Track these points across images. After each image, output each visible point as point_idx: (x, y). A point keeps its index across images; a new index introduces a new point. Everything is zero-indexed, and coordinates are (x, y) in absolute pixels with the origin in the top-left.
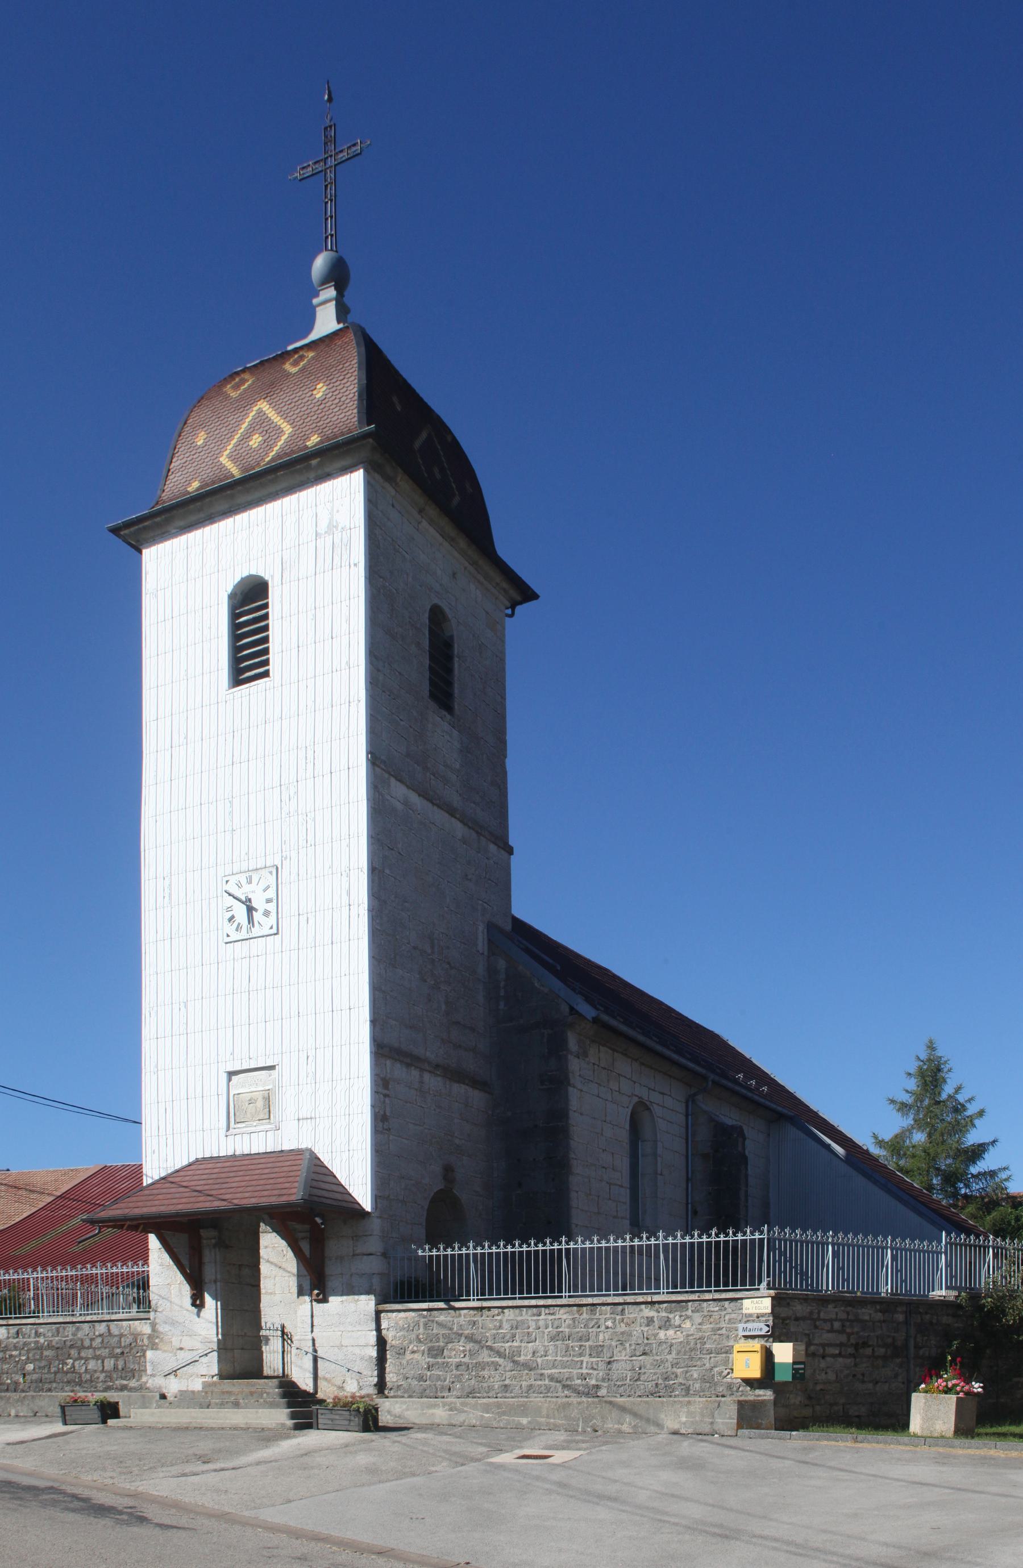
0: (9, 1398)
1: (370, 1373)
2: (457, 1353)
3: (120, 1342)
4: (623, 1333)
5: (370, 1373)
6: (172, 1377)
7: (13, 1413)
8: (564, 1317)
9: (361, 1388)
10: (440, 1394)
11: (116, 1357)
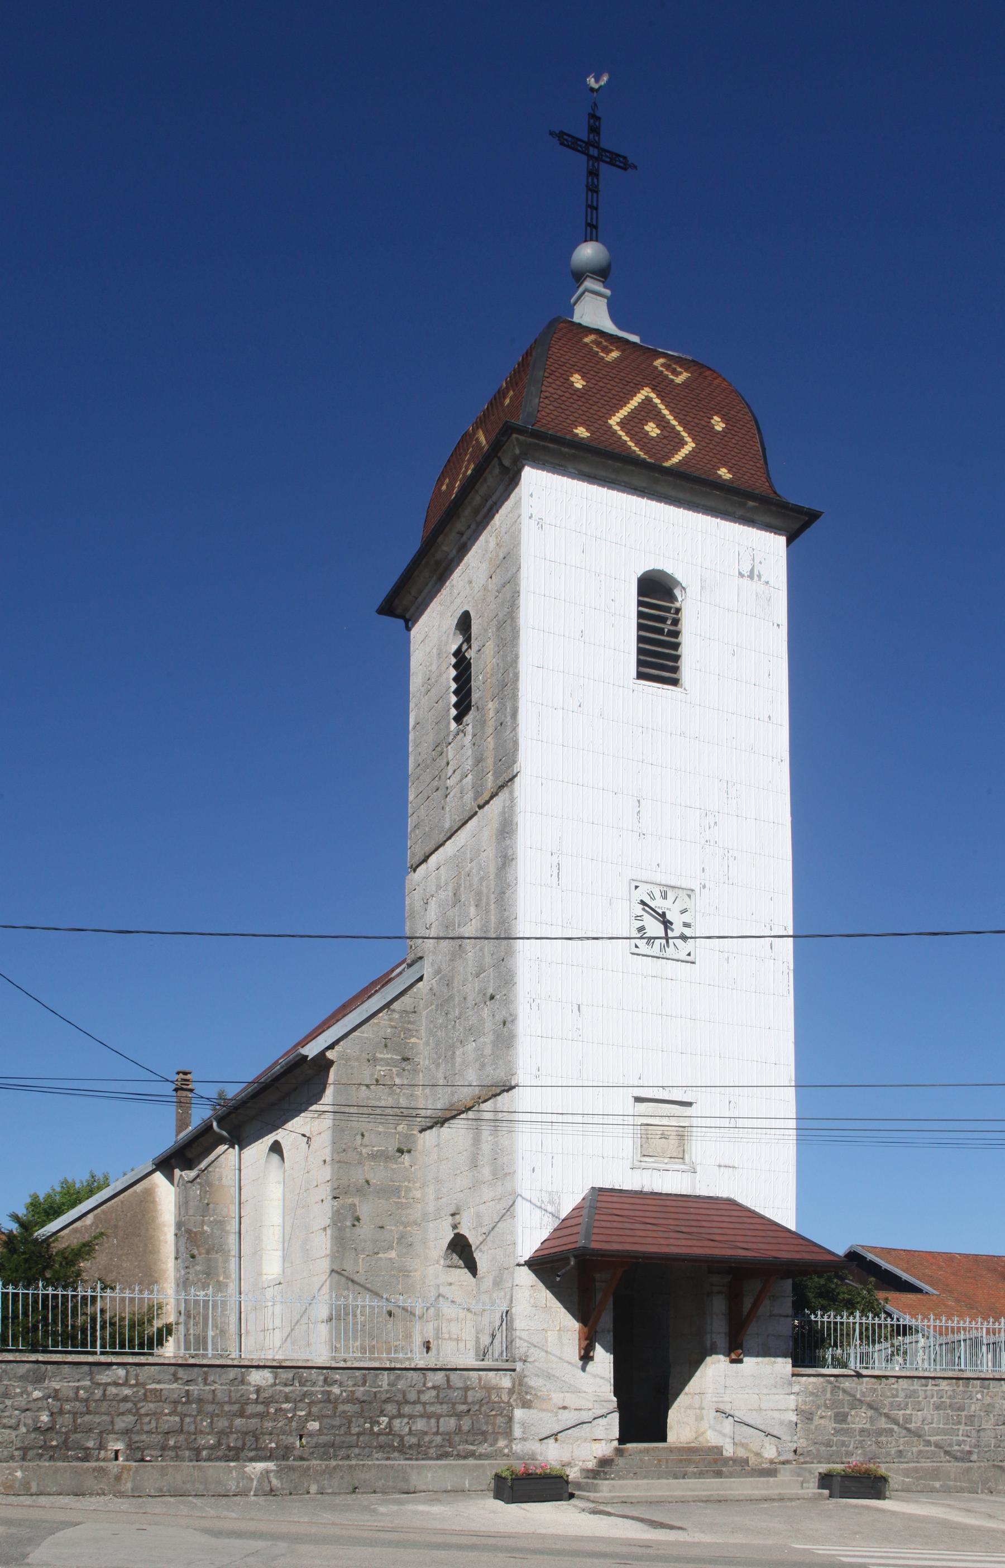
0: (308, 1468)
1: (789, 1439)
2: (860, 1419)
3: (466, 1397)
4: (989, 1405)
5: (789, 1439)
6: (551, 1441)
7: (314, 1488)
8: (947, 1388)
9: (779, 1454)
10: (844, 1460)
11: (459, 1416)
